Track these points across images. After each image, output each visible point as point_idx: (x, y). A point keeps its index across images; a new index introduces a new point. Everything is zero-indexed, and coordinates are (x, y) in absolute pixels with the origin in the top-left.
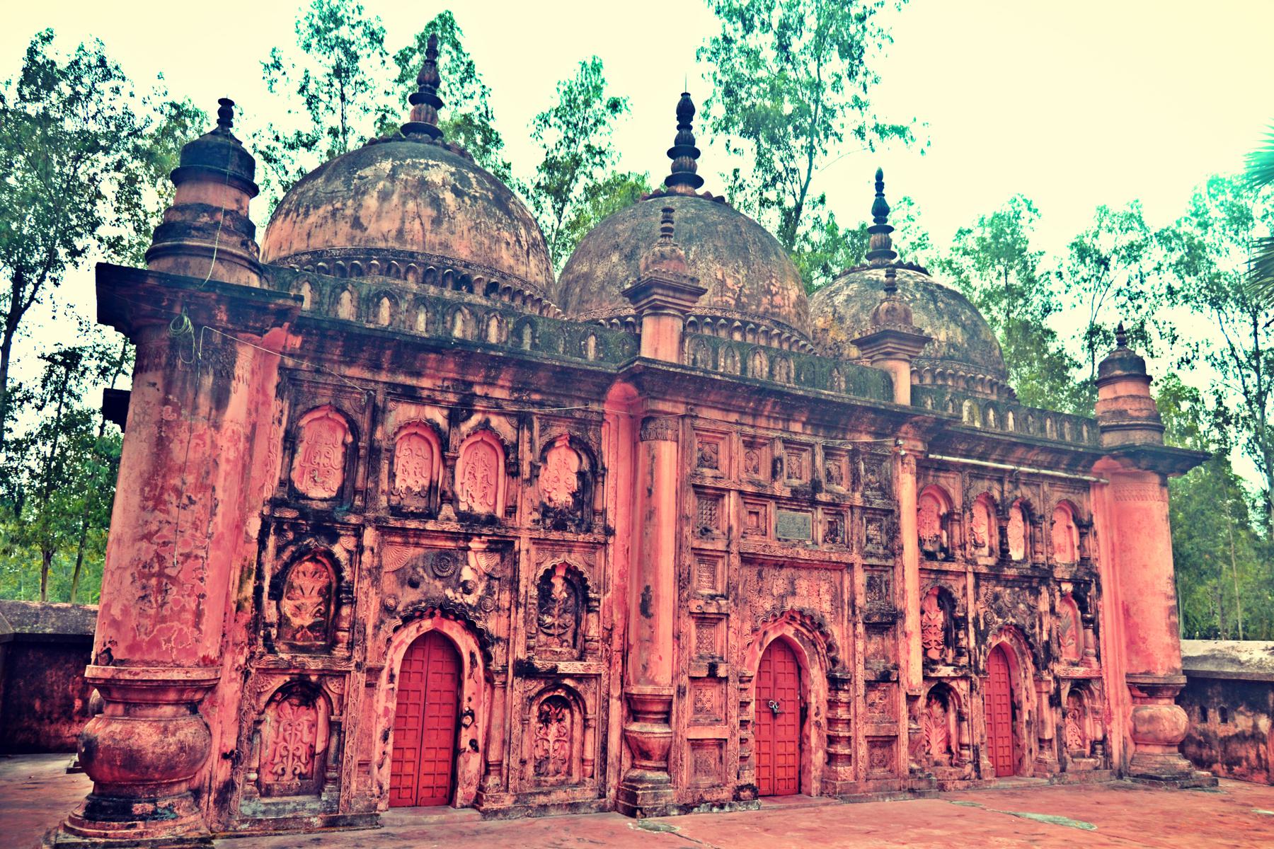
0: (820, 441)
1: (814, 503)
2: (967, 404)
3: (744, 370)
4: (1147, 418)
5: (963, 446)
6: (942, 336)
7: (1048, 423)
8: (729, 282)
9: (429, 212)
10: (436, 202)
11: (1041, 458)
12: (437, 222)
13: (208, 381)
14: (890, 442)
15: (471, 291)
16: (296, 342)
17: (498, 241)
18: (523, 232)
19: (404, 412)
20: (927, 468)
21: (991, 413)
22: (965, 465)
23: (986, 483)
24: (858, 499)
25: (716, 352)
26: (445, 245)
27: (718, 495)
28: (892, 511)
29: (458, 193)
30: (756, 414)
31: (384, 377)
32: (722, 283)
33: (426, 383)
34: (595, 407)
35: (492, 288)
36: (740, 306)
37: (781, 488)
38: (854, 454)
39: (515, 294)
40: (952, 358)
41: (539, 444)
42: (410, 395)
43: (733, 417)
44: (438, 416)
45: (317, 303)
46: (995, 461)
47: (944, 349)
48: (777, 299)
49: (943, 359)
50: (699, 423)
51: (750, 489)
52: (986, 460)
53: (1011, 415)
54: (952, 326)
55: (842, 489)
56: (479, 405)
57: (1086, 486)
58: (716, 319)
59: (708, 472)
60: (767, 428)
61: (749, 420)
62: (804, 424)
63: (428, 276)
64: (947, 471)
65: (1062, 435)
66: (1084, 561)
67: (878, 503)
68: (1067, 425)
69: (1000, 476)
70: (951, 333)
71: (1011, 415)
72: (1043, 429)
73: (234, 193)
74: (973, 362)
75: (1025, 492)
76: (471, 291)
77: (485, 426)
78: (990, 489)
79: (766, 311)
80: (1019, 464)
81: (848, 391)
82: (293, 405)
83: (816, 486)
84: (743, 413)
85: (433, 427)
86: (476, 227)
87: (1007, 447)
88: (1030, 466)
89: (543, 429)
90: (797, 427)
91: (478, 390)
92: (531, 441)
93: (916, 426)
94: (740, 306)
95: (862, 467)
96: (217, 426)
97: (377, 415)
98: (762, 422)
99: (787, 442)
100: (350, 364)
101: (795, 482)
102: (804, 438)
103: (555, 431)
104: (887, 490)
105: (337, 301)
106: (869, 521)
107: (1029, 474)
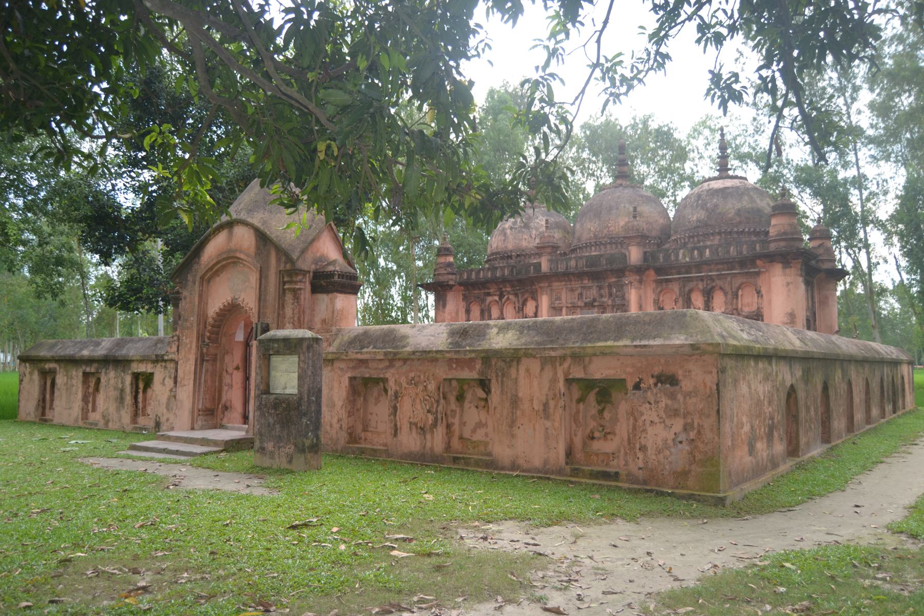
0: (596, 284)
1: (594, 306)
2: (682, 251)
3: (567, 267)
4: (776, 236)
5: (674, 271)
6: (695, 218)
7: (732, 248)
8: (592, 228)
9: (503, 238)
10: (505, 235)
11: (720, 267)
12: (504, 240)
13: (441, 303)
14: (623, 279)
15: (511, 259)
16: (462, 288)
17: (522, 240)
18: (534, 232)
19: (489, 299)
20: (661, 282)
21: (696, 252)
22: (680, 278)
23: (695, 283)
24: (610, 302)
25: (557, 263)
26: (506, 247)
27: (561, 309)
28: (624, 305)
29: (511, 228)
30: (570, 281)
31: (483, 291)
32: (590, 229)
33: (492, 291)
34: (534, 287)
35: (518, 256)
36: (595, 236)
37: (580, 303)
38: (610, 286)
39: (525, 256)
40: (698, 227)
41: (521, 301)
42: (489, 294)
43: (563, 283)
44: (497, 298)
45: (468, 276)
46: (696, 273)
47: (695, 224)
48: (612, 228)
49: (694, 228)
50: (553, 288)
51: (570, 305)
52: (691, 273)
53: (707, 250)
54: (701, 211)
55: (605, 300)
56: (505, 294)
57: (758, 274)
58: (590, 243)
59: (557, 302)
60: (576, 284)
61: (569, 283)
62: (589, 280)
63: (502, 258)
64: (671, 281)
65: (741, 253)
66: (758, 308)
67: (618, 302)
68: (745, 246)
69: (702, 279)
70: (699, 215)
71: (707, 250)
72: (728, 252)
73: (444, 258)
74: (710, 225)
75: (718, 283)
76: (511, 259)
77: (508, 298)
78: (697, 285)
79: (606, 235)
80: (711, 271)
81: (606, 264)
82: (467, 302)
83: (594, 300)
84: (566, 281)
85: (496, 301)
86: (515, 238)
87: (699, 266)
88: (717, 270)
89: (523, 296)
90: (586, 282)
91: (503, 289)
92: (518, 301)
93: (629, 271)
94: (595, 236)
95: (614, 290)
96: (444, 312)
97: (483, 301)
98: (573, 283)
99: (583, 288)
100: (475, 290)
101: (588, 300)
102: (590, 285)
103: (525, 297)
104: (623, 298)
105: (471, 274)
106: (617, 309)
107: (718, 275)
